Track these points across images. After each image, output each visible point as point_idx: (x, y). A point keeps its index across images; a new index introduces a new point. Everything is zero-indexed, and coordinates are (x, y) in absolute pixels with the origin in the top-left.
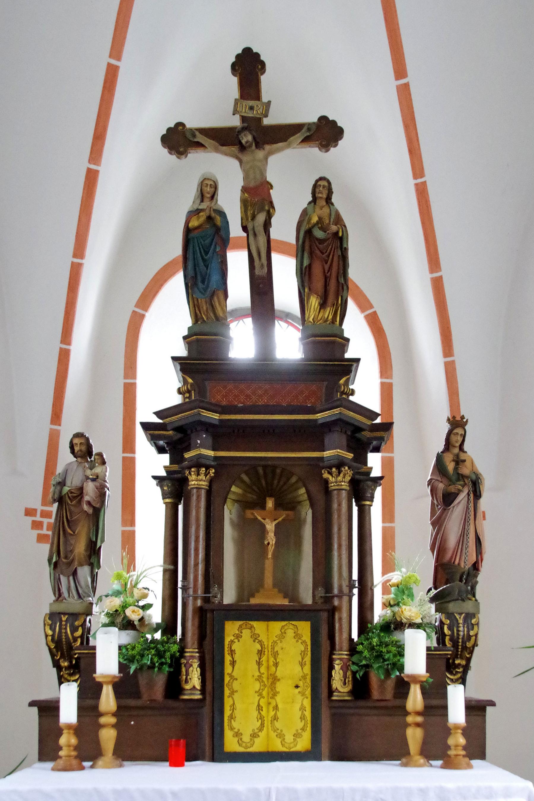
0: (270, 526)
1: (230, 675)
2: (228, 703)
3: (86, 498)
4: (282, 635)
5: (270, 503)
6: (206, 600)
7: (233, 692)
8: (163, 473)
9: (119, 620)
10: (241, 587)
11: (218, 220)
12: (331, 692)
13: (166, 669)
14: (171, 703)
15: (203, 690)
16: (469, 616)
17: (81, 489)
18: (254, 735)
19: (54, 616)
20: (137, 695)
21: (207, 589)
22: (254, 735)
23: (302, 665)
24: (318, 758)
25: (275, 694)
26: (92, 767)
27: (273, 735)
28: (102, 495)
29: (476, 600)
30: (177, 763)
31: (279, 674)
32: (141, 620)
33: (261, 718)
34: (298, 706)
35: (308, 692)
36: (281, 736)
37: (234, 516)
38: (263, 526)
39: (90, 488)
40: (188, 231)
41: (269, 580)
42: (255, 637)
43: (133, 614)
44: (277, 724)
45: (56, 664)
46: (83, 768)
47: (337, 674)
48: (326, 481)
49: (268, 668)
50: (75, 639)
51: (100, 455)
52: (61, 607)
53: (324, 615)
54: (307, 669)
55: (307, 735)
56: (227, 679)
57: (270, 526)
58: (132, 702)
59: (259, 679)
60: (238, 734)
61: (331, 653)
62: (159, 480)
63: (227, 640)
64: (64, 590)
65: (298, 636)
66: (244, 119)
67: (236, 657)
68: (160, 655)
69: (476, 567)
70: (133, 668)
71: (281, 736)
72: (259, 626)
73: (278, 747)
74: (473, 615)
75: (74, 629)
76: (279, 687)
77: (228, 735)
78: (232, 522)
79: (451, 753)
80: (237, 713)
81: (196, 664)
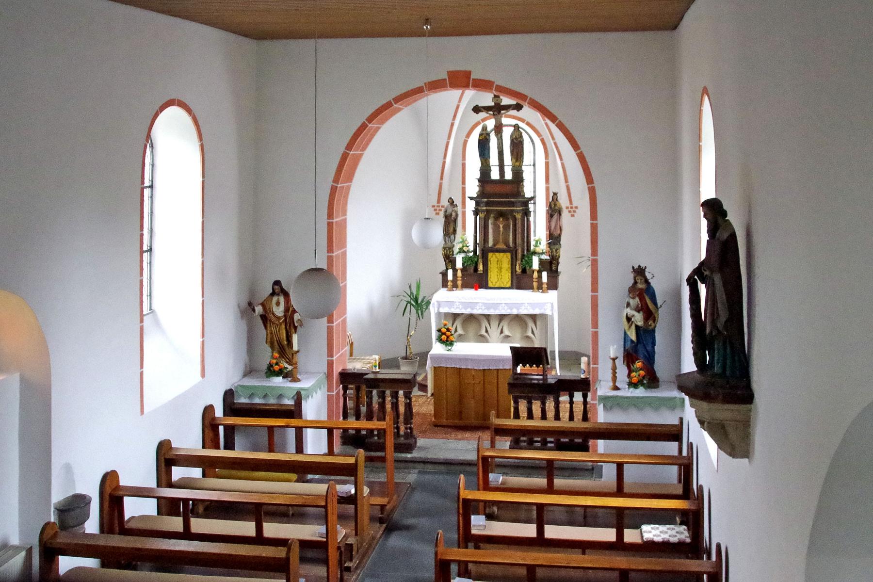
0: (501, 226)
1: (490, 267)
2: (489, 274)
3: (453, 217)
4: (503, 257)
5: (501, 219)
6: (484, 247)
7: (491, 271)
8: (474, 209)
9: (461, 251)
10: (494, 240)
11: (487, 137)
12: (516, 271)
13: (474, 265)
14: (475, 274)
15: (483, 271)
16: (557, 250)
17: (451, 214)
18: (496, 283)
19: (444, 248)
20: (467, 271)
21: (484, 244)
22: (496, 283)
23: (508, 264)
24: (513, 289)
25: (501, 272)
26: (456, 290)
27: (501, 283)
28: (457, 215)
29: (560, 244)
30: (476, 289)
31: (502, 267)
32: (468, 251)
33: (498, 278)
34: (507, 275)
35: (510, 272)
36: (503, 283)
37: (492, 222)
38: (499, 225)
39: (454, 214)
40: (479, 140)
41: (501, 241)
42: (496, 257)
43: (465, 249)
44: (502, 280)
45: (445, 261)
46: (453, 290)
47: (517, 267)
48: (515, 216)
49: (500, 265)
50: (450, 255)
51: (456, 205)
52: (447, 246)
53: (514, 251)
54: (510, 266)
55: (510, 282)
56: (489, 268)
57: (501, 226)
58: (465, 273)
59: (497, 268)
60: (492, 282)
61: (516, 261)
62: (473, 211)
63: (489, 258)
64: (447, 242)
65: (507, 257)
66: (495, 103)
67: (492, 262)
68: (472, 261)
69: (560, 235)
70: (465, 265)
71: (503, 283)
72: (497, 254)
73: (503, 286)
74: (558, 249)
75: (450, 252)
76: (502, 270)
77: (489, 282)
78: (491, 224)
79: (543, 289)
80: (492, 277)
81: (481, 264)
